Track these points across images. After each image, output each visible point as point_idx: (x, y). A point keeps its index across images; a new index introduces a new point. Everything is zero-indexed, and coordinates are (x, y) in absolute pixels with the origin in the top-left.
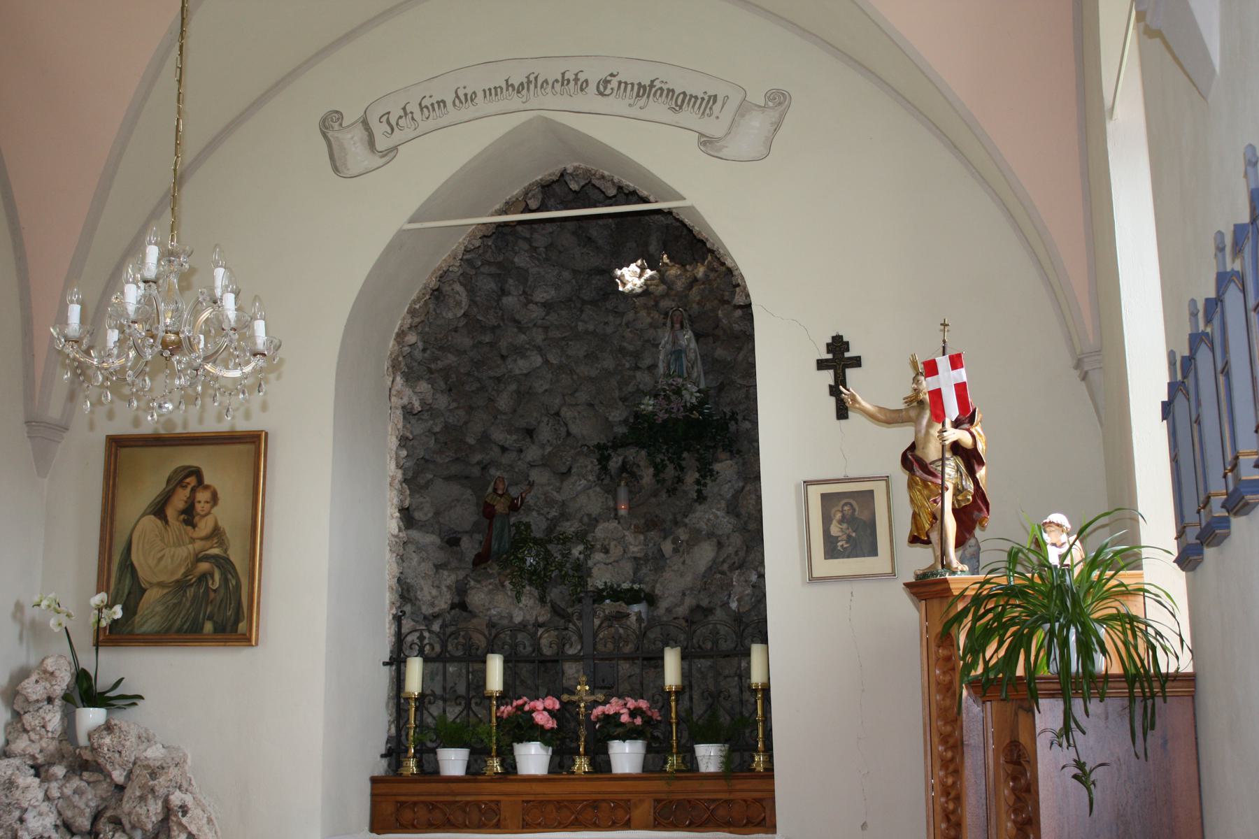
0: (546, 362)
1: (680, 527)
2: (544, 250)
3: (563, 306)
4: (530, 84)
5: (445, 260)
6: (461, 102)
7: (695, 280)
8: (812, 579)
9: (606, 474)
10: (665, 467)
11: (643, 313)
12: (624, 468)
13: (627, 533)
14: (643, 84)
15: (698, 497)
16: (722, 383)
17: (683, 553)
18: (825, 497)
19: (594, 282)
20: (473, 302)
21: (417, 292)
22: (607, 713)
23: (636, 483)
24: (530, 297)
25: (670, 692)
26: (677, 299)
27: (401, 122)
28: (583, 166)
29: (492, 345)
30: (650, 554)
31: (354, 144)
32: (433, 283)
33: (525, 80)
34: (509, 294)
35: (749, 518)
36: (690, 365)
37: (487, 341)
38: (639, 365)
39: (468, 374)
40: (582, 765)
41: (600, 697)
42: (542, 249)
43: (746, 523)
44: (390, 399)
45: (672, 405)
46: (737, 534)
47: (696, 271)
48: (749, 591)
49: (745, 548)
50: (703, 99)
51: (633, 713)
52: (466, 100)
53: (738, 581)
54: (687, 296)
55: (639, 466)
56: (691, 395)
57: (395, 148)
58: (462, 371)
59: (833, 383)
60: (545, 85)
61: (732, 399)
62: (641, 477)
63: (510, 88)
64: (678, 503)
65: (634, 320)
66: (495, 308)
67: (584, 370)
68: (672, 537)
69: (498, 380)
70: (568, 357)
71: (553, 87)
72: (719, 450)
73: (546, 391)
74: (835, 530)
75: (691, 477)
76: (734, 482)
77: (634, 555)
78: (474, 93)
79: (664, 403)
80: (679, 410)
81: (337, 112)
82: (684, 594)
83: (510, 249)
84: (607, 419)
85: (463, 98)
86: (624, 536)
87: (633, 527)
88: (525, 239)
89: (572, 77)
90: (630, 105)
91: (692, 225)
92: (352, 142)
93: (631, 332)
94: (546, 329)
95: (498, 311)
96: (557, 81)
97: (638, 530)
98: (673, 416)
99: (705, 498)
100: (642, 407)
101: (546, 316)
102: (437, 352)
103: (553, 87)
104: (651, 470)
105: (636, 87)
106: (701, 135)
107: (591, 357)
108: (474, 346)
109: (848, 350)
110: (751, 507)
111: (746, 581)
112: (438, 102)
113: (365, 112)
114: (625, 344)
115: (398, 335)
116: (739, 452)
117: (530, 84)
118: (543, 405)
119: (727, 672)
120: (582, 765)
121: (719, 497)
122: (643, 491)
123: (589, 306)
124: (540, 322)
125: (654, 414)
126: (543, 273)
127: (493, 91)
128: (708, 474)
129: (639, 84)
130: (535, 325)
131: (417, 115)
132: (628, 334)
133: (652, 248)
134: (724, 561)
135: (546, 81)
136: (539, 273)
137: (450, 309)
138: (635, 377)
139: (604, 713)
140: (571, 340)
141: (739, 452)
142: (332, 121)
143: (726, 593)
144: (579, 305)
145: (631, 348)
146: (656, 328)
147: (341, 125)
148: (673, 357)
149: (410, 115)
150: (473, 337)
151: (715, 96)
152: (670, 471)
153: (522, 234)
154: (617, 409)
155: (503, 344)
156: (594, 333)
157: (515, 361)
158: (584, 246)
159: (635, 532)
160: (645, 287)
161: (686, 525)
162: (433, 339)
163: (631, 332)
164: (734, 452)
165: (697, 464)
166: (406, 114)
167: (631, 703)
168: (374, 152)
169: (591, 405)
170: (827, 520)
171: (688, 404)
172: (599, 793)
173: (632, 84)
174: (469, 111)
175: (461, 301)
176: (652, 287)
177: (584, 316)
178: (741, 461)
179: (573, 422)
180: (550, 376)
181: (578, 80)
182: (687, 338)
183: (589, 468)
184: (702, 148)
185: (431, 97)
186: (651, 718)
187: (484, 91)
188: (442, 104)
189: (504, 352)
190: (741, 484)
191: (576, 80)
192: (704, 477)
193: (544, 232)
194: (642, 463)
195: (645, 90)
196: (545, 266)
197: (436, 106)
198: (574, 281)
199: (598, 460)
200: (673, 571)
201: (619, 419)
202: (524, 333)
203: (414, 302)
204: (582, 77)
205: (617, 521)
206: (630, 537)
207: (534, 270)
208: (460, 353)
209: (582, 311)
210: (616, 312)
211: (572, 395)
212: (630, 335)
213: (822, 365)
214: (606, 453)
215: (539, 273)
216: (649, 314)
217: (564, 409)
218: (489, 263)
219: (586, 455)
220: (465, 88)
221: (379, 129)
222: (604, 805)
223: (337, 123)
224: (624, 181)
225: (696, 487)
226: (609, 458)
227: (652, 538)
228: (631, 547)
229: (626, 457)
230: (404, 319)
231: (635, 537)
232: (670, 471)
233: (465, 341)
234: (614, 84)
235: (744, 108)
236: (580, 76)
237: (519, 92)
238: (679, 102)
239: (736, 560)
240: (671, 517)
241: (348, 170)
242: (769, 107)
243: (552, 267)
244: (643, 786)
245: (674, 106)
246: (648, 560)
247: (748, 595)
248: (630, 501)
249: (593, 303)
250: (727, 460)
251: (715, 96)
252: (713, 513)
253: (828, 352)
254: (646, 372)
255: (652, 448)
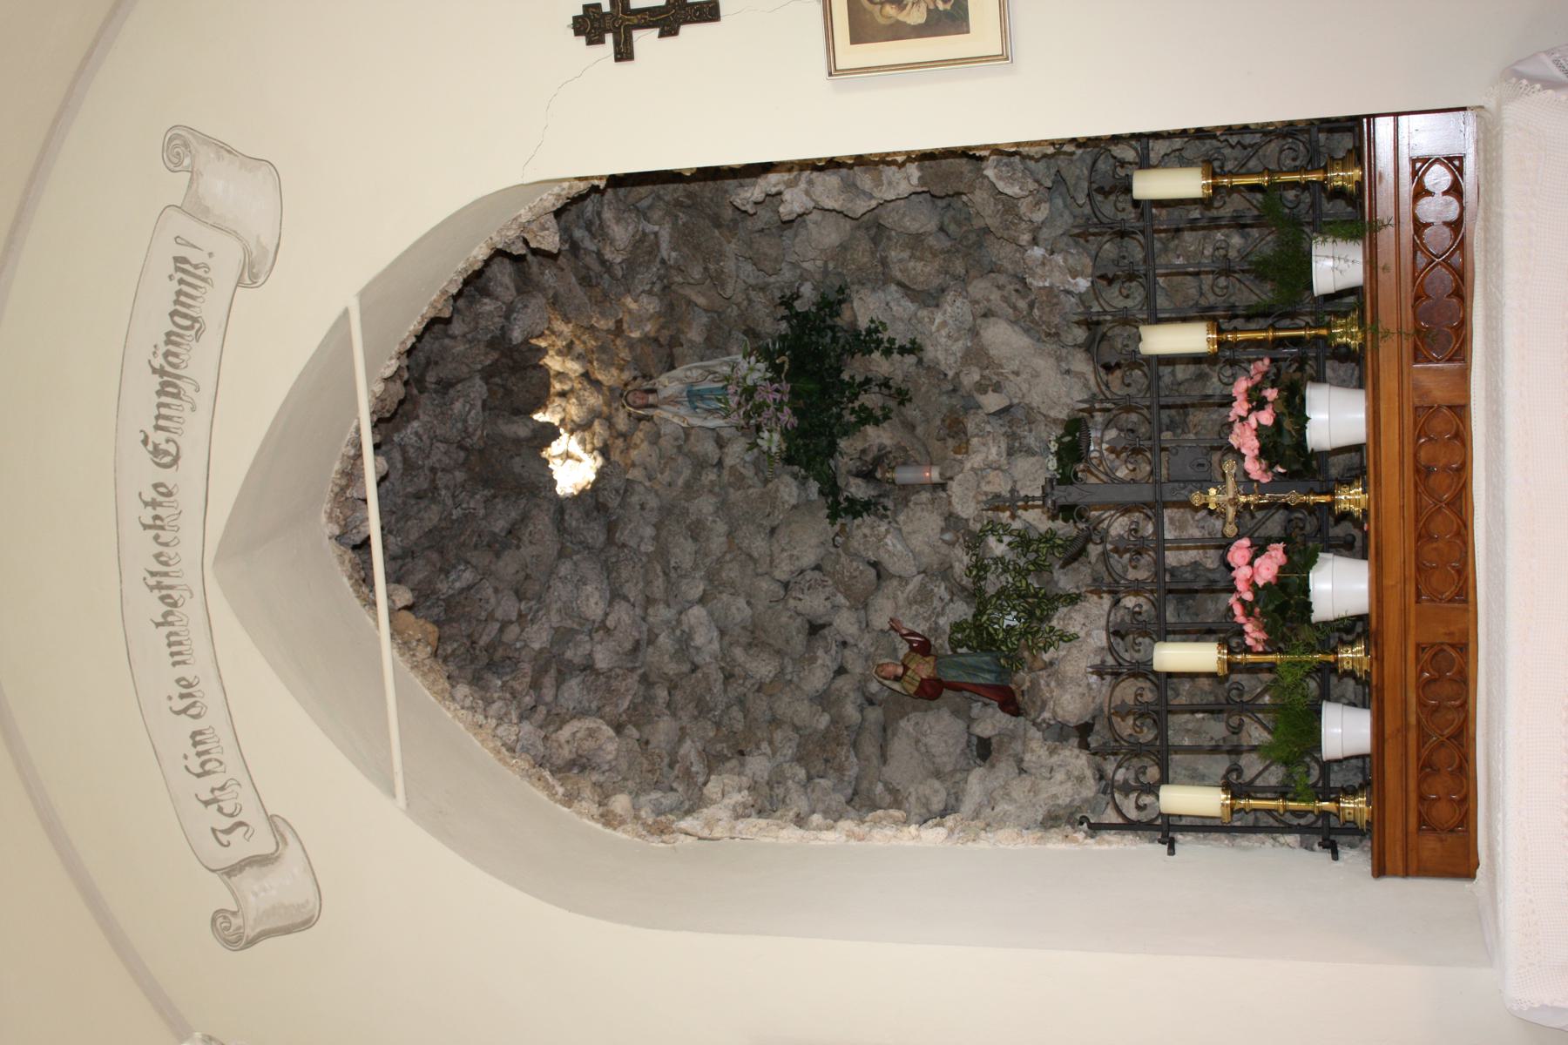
0: (702, 600)
1: (960, 383)
2: (523, 603)
3: (614, 575)
4: (162, 585)
5: (483, 742)
6: (193, 705)
7: (586, 375)
8: (1004, 56)
9: (876, 504)
10: (863, 408)
11: (634, 454)
12: (867, 475)
13: (968, 465)
14: (158, 388)
15: (911, 351)
16: (745, 333)
17: (1002, 374)
18: (856, 38)
19: (574, 523)
20: (599, 713)
21: (534, 790)
22: (1256, 452)
23: (891, 456)
24: (596, 625)
25: (1220, 343)
26: (615, 405)
27: (228, 809)
28: (326, 507)
29: (673, 687)
30: (1003, 430)
31: (265, 890)
32: (521, 763)
33: (157, 593)
34: (590, 655)
35: (947, 273)
36: (711, 377)
37: (666, 693)
38: (715, 462)
39: (718, 725)
40: (1351, 498)
41: (1229, 466)
42: (523, 606)
43: (955, 278)
44: (718, 839)
45: (770, 401)
46: (970, 289)
47: (573, 375)
48: (1059, 259)
49: (993, 275)
50: (181, 281)
51: (1258, 404)
52: (190, 695)
53: (1043, 278)
54: (611, 389)
55: (863, 451)
56: (755, 371)
57: (271, 819)
58: (711, 734)
59: (656, 31)
60: (163, 559)
61: (768, 315)
62: (881, 447)
63: (170, 619)
64: (923, 389)
65: (645, 469)
66: (609, 677)
67: (717, 544)
68: (976, 395)
69: (728, 677)
70: (695, 567)
71: (166, 544)
72: (838, 321)
73: (748, 603)
74: (916, 16)
75: (880, 364)
76: (889, 298)
77: (1004, 455)
78: (178, 681)
79: (767, 413)
80: (777, 390)
81: (214, 920)
82: (1068, 372)
83: (516, 655)
84: (795, 507)
85: (188, 701)
86: (973, 469)
87: (959, 457)
88: (501, 630)
89: (150, 512)
90: (193, 409)
91: (419, 318)
92: (262, 894)
93: (662, 473)
94: (649, 601)
95: (613, 673)
96: (156, 538)
97: (964, 448)
98: (786, 399)
99: (913, 342)
100: (774, 450)
101: (629, 601)
102: (676, 772)
103: (166, 544)
104: (870, 429)
105: (164, 399)
106: (239, 283)
107: (696, 531)
108: (674, 715)
109: (598, 6)
110: (927, 269)
111: (1043, 264)
112: (195, 744)
113: (213, 871)
114: (680, 482)
115: (607, 824)
116: (841, 290)
117: (162, 585)
118: (770, 608)
119: (1193, 292)
120: (1351, 498)
121: (914, 321)
122: (903, 444)
123: (617, 535)
124: (638, 611)
125: (785, 433)
126: (559, 604)
127: (175, 649)
128: (874, 337)
129: (159, 393)
130: (644, 619)
131: (216, 780)
132: (666, 477)
133: (523, 431)
134: (1015, 308)
135: (157, 556)
136: (559, 611)
137: (600, 748)
138: (731, 467)
139: (1259, 457)
140: (668, 562)
141: (841, 290)
142: (227, 929)
143: (1062, 296)
144: (614, 550)
145: (687, 473)
146: (658, 435)
147: (234, 914)
148: (699, 404)
149: (217, 793)
150: (659, 717)
151: (176, 259)
152: (872, 399)
153: (493, 634)
154: (777, 490)
155: (671, 668)
156: (658, 526)
157: (698, 649)
158: (519, 539)
159: (966, 453)
160: (596, 453)
161: (957, 374)
162: (650, 776)
163: (662, 473)
164: (841, 297)
165: (858, 356)
166: (215, 800)
167: (1240, 407)
168: (278, 857)
169: (773, 531)
170: (898, 32)
171: (769, 375)
172: (1402, 463)
173: (160, 405)
174: (208, 692)
175: (588, 729)
176: (595, 441)
177: (633, 543)
178: (855, 287)
179: (798, 558)
180: (725, 597)
181: (154, 500)
182: (669, 384)
183: (867, 531)
184: (261, 281)
185: (186, 757)
186: (1265, 375)
187: (175, 664)
188: (198, 738)
189: (686, 668)
190: (893, 287)
191: (154, 504)
192: (879, 342)
193: (493, 600)
194: (860, 445)
195: (169, 384)
196: (548, 601)
197: (201, 748)
198: (575, 558)
199: (854, 518)
200: (1029, 391)
201: (794, 489)
202: (657, 636)
203: (553, 795)
204: (149, 494)
205: (950, 483)
206: (976, 460)
207: (555, 619)
208: (683, 734)
209: (624, 545)
210: (626, 491)
211: (755, 561)
212: (666, 474)
213: (624, 53)
214: (845, 504)
215: (559, 611)
216: (636, 446)
217: (778, 574)
218: (535, 685)
219: (848, 538)
220: (170, 698)
221: (241, 847)
222: (1422, 454)
223: (232, 919)
224: (348, 437)
225: (896, 356)
226: (851, 501)
227: (978, 425)
228: (990, 458)
229: (849, 472)
230: (579, 813)
231: (974, 452)
232: (872, 399)
233: (663, 730)
234: (159, 438)
235: (195, 209)
236: (148, 499)
237: (175, 605)
238: (187, 323)
239: (1012, 287)
240: (944, 398)
241: (307, 902)
242: (193, 162)
243: (551, 590)
244: (1389, 383)
245: (193, 333)
246: (1014, 433)
247: (1065, 260)
248: (917, 463)
249: (611, 528)
250: (852, 308)
251: (176, 259)
252: (938, 331)
253: (602, 41)
254: (726, 450)
255: (835, 431)
